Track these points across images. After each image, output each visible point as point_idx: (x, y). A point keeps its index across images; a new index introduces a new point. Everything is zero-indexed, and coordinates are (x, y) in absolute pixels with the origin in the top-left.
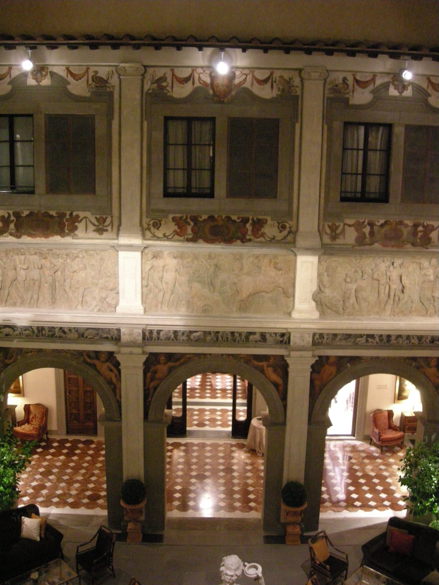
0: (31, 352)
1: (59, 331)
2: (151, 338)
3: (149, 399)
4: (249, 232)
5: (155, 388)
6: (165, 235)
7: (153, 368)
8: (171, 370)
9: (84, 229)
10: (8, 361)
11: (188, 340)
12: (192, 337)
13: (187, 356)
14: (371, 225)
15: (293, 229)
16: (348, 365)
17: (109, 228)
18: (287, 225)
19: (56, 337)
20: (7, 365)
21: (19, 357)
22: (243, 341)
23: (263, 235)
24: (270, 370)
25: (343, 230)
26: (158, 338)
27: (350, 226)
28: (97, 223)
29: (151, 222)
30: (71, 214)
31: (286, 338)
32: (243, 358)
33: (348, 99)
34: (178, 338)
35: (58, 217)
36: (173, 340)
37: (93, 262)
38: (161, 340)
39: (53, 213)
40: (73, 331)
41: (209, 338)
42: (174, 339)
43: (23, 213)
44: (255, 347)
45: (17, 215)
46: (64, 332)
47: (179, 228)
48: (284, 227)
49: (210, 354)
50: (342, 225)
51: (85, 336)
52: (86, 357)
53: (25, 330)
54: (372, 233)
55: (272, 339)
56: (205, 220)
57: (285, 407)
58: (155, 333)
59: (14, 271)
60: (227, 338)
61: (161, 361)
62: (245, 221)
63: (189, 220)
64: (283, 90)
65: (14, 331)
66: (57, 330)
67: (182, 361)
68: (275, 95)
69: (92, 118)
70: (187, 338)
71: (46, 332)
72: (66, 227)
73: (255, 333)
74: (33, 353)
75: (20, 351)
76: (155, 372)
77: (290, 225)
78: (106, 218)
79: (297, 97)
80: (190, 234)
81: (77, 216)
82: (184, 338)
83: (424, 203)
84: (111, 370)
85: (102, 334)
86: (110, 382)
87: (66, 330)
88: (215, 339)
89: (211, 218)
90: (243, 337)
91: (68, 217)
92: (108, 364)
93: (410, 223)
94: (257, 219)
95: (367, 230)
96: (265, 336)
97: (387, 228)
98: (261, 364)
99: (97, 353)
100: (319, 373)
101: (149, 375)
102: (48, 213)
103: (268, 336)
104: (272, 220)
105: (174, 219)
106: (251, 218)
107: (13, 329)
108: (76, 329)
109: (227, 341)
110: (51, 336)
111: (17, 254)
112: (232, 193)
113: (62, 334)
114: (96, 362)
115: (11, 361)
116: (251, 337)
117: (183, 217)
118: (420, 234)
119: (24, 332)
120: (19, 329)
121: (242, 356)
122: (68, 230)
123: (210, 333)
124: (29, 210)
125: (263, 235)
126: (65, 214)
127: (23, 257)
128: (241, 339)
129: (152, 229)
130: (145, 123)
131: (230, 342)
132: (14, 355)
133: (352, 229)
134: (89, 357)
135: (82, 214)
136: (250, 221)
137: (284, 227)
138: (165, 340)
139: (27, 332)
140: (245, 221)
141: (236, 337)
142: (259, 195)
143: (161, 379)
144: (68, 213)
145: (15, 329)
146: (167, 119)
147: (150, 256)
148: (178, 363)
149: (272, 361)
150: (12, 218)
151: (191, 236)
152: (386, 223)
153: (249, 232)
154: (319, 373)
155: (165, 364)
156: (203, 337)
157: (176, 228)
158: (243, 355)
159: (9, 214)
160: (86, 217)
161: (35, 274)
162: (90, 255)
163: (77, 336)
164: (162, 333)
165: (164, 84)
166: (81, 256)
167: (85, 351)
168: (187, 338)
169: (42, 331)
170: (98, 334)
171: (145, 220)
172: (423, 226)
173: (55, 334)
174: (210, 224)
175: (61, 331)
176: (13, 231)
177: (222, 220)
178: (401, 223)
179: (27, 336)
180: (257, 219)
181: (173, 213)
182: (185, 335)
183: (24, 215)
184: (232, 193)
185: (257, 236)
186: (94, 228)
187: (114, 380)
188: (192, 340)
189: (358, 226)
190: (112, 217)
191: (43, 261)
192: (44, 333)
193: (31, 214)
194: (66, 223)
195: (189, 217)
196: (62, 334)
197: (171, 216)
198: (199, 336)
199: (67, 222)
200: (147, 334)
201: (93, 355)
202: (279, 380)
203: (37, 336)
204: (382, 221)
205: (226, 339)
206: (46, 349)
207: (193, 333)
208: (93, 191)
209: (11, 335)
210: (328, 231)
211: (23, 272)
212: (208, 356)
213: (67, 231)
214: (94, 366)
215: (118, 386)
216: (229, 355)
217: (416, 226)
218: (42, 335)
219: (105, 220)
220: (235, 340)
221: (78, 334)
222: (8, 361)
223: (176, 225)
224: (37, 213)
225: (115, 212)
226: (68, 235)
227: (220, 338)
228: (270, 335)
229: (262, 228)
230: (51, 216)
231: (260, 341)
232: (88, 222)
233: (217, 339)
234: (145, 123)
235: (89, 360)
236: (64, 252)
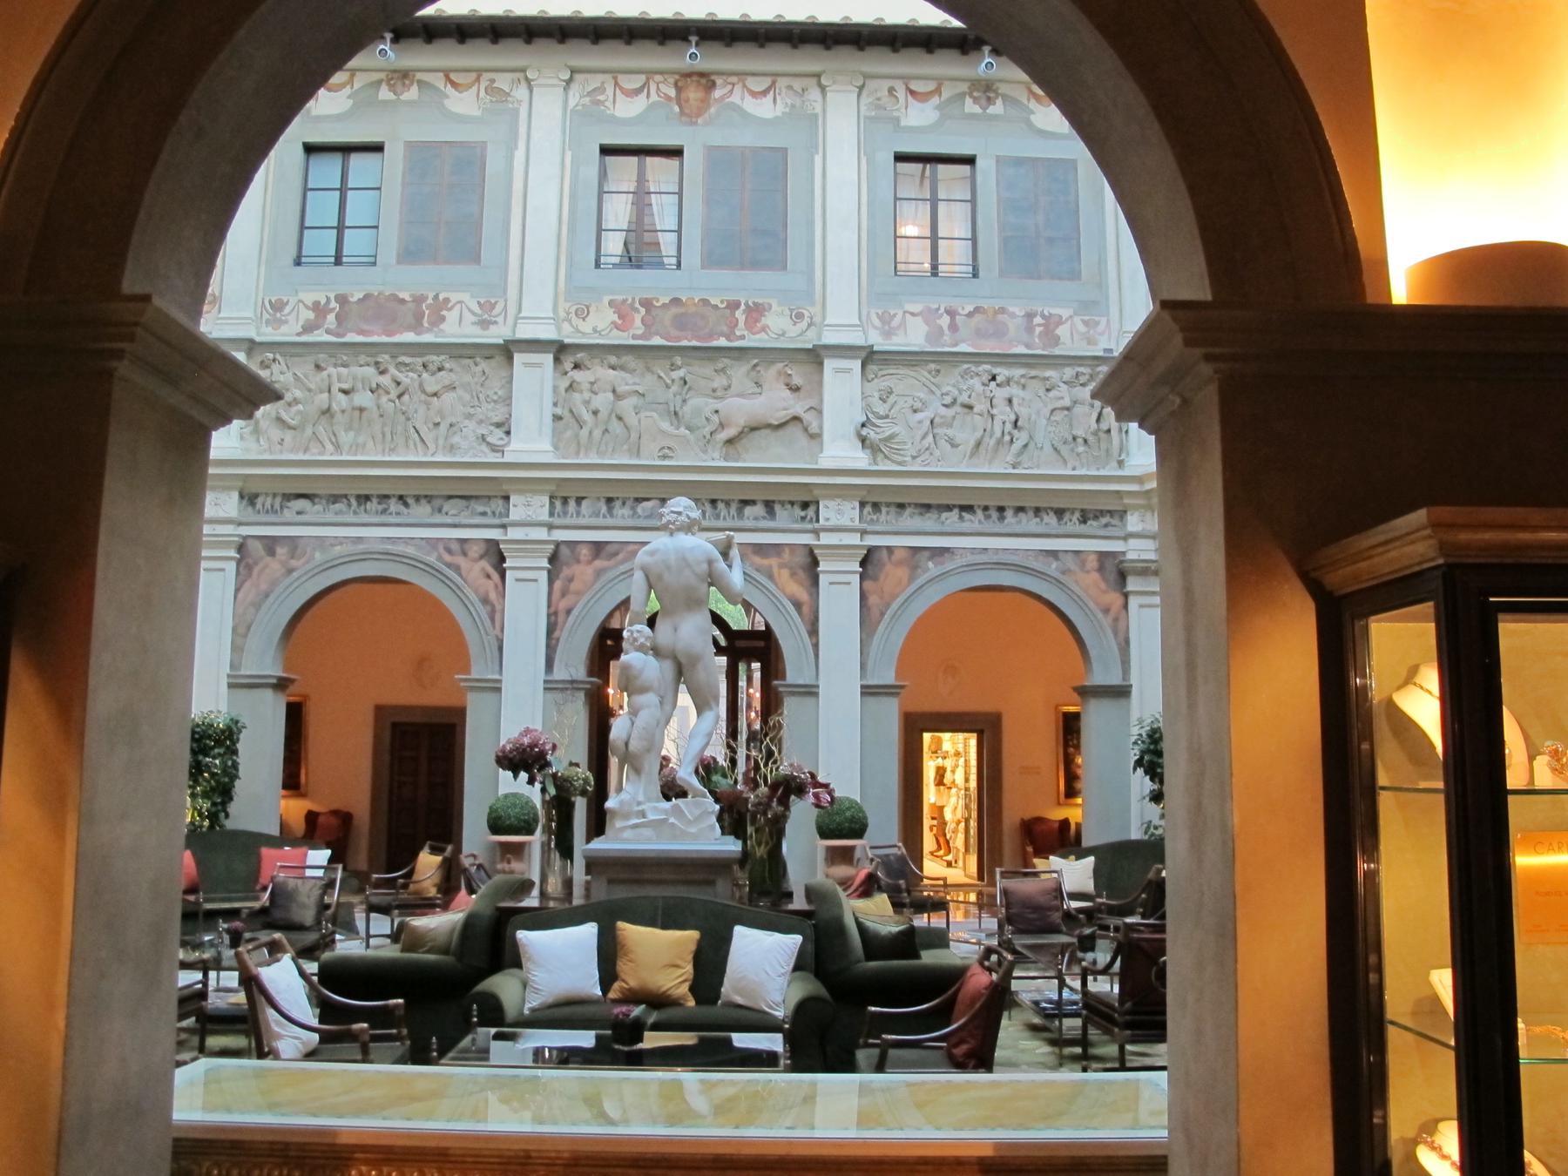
3: (556, 634)
4: (741, 324)
5: (569, 612)
6: (595, 330)
7: (566, 572)
8: (599, 573)
10: (294, 563)
14: (951, 313)
15: (817, 319)
16: (930, 564)
20: (290, 571)
23: (764, 329)
24: (785, 573)
25: (903, 323)
27: (913, 314)
28: (477, 309)
29: (573, 310)
30: (436, 297)
33: (898, 120)
39: (405, 295)
45: (342, 300)
48: (800, 316)
50: (900, 313)
52: (441, 550)
54: (953, 327)
57: (816, 646)
61: (582, 558)
62: (734, 305)
64: (793, 106)
67: (620, 556)
68: (779, 114)
69: (483, 145)
71: (373, 505)
76: (571, 580)
79: (816, 116)
81: (447, 300)
83: (1039, 278)
84: (488, 576)
86: (485, 601)
89: (676, 301)
91: (430, 301)
93: (1019, 312)
95: (945, 321)
97: (978, 317)
98: (765, 562)
99: (463, 541)
100: (875, 579)
101: (558, 584)
104: (780, 304)
105: (611, 303)
112: (712, 260)
118: (1038, 330)
125: (764, 329)
129: (575, 321)
130: (569, 154)
133: (919, 319)
134: (449, 551)
135: (454, 297)
137: (800, 316)
140: (734, 305)
142: (756, 265)
143: (579, 594)
144: (431, 295)
146: (606, 151)
147: (568, 365)
148: (612, 562)
149: (786, 555)
150: (333, 304)
151: (640, 332)
152: (977, 310)
153: (741, 324)
154: (875, 579)
155: (590, 562)
157: (615, 317)
159: (328, 299)
161: (363, 398)
165: (601, 98)
171: (563, 306)
172: (1043, 316)
174: (675, 310)
176: (333, 326)
178: (1002, 310)
184: (712, 260)
186: (475, 319)
187: (493, 596)
189: (929, 315)
193: (367, 297)
197: (606, 299)
201: (455, 547)
202: (803, 596)
204: (970, 308)
210: (877, 322)
211: (341, 396)
214: (457, 569)
215: (498, 607)
217: (1030, 316)
219: (493, 306)
222: (294, 563)
226: (429, 330)
230: (403, 301)
232: (465, 311)
234: (569, 154)
235: (448, 558)
236: (419, 360)
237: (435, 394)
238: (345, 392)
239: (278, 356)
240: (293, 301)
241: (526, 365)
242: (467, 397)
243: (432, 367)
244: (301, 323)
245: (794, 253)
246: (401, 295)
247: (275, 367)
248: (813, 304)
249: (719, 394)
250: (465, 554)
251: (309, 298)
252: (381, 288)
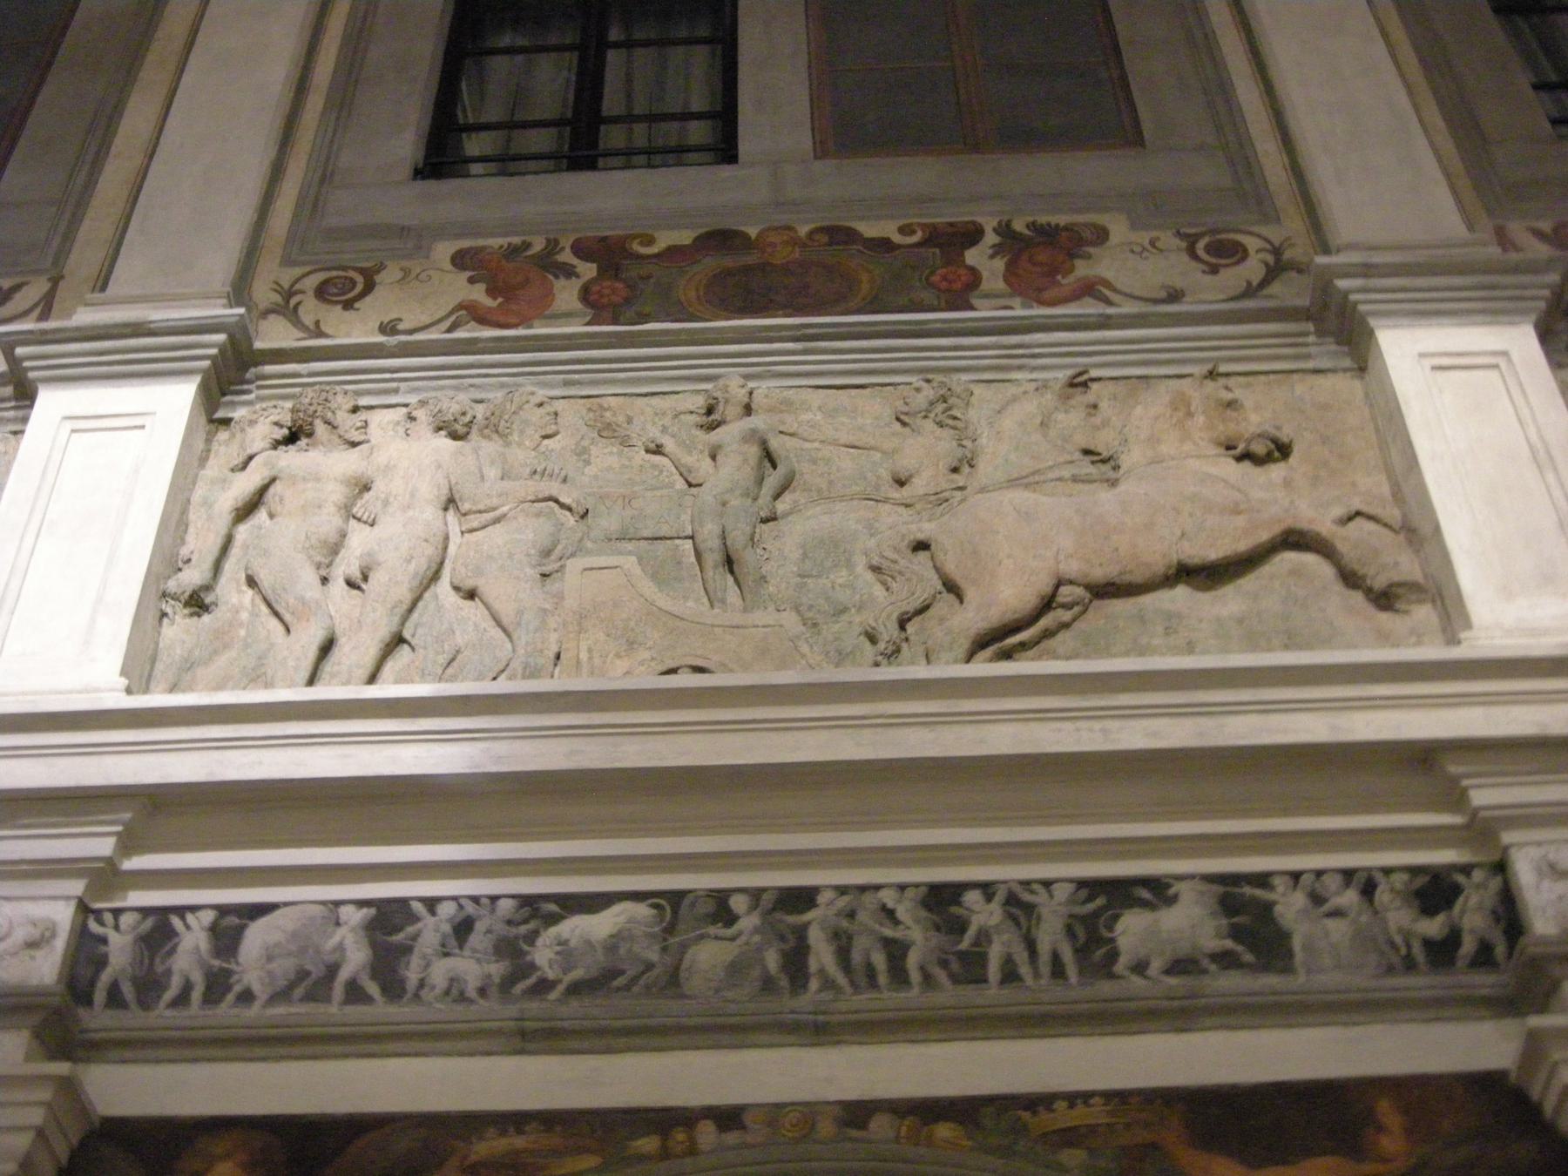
2: (149, 986)
11: (508, 983)
12: (543, 954)
13: (488, 1147)
18: (1251, 243)
22: (1058, 971)
26: (218, 984)
31: (1473, 914)
32: (1069, 1137)
34: (412, 976)
36: (355, 993)
38: (247, 997)
41: (709, 955)
42: (373, 989)
44: (1182, 1016)
47: (492, 292)
49: (728, 1118)
55: (1337, 927)
56: (673, 252)
58: (193, 939)
60: (896, 951)
63: (567, 257)
70: (497, 969)
73: (1158, 891)
77: (1266, 240)
80: (568, 315)
82: (471, 967)
88: (772, 960)
90: (1050, 934)
94: (1032, 226)
96: (1265, 910)
103: (1290, 907)
106: (989, 225)
109: (899, 975)
116: (1131, 929)
117: (527, 245)
121: (1064, 1118)
123: (720, 908)
128: (1031, 946)
131: (927, 978)
136: (991, 238)
138: (281, 996)
141: (984, 937)
156: (653, 955)
157: (478, 294)
158: (1075, 1098)
164: (257, 936)
168: (497, 969)
177: (795, 242)
180: (1032, 226)
181: (458, 236)
182: (477, 939)
185: (1047, 295)
188: (544, 986)
190: (55, 282)
195: (566, 242)
197: (444, 251)
198: (613, 944)
200: (120, 946)
205: (879, 960)
207: (553, 919)
212: (707, 1134)
216: (928, 1111)
220: (971, 968)
223: (471, 281)
227: (822, 955)
228: (1317, 899)
229: (1078, 263)
231: (1226, 960)
233: (796, 961)
245: (1152, 71)
248: (1270, 216)
249: (919, 486)
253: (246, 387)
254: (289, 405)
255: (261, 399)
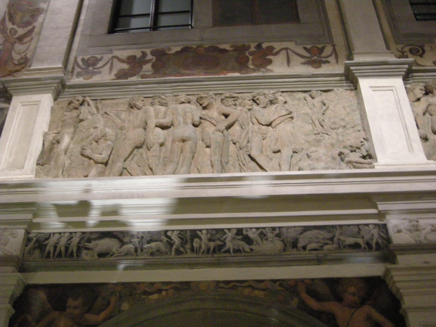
0: (159, 291)
1: (234, 239)
9: (285, 62)
17: (332, 59)
19: (228, 251)
21: (125, 306)
28: (308, 55)
30: (259, 46)
35: (234, 51)
37: (306, 110)
40: (270, 235)
43: (170, 49)
46: (248, 240)
51: (301, 244)
52: (304, 295)
53: (149, 242)
59: (142, 130)
65: (123, 243)
66: (229, 235)
71: (203, 242)
72: (250, 62)
74: (164, 293)
75: (130, 289)
78: (323, 48)
85: (342, 238)
87: (252, 235)
91: (253, 49)
92: (367, 309)
99: (333, 283)
102: (218, 47)
107: (118, 238)
108: (277, 231)
110: (214, 251)
111: (152, 104)
113: (243, 244)
114: (332, 306)
115: (103, 315)
119: (146, 246)
120: (136, 240)
122: (254, 64)
124: (181, 45)
126: (249, 47)
127: (163, 109)
132: (113, 300)
135: (277, 46)
139: (153, 244)
144: (253, 46)
145: (126, 240)
150: (149, 57)
160: (286, 49)
161: (188, 131)
162: (300, 99)
163: (279, 245)
166: (281, 98)
167: (302, 281)
169: (192, 241)
170: (332, 239)
173: (225, 244)
175: (240, 237)
179: (152, 254)
183: (172, 52)
191: (205, 112)
192: (196, 245)
193: (185, 50)
194: (251, 57)
196: (242, 243)
199: (250, 55)
201: (324, 290)
203: (178, 252)
206: (199, 282)
208: (296, 19)
209: (114, 254)
213: (251, 67)
218: (192, 249)
219: (321, 50)
221: (283, 241)
224: (198, 47)
225: (339, 40)
232: (290, 53)
237: (269, 125)
238: (164, 127)
239: (88, 99)
240: (107, 57)
241: (375, 88)
242: (309, 127)
243: (263, 100)
244: (114, 72)
246: (222, 47)
247: (84, 109)
250: (339, 299)
251: (124, 54)
252: (199, 43)
253: (409, 79)
254: (424, 84)
255: (413, 82)
